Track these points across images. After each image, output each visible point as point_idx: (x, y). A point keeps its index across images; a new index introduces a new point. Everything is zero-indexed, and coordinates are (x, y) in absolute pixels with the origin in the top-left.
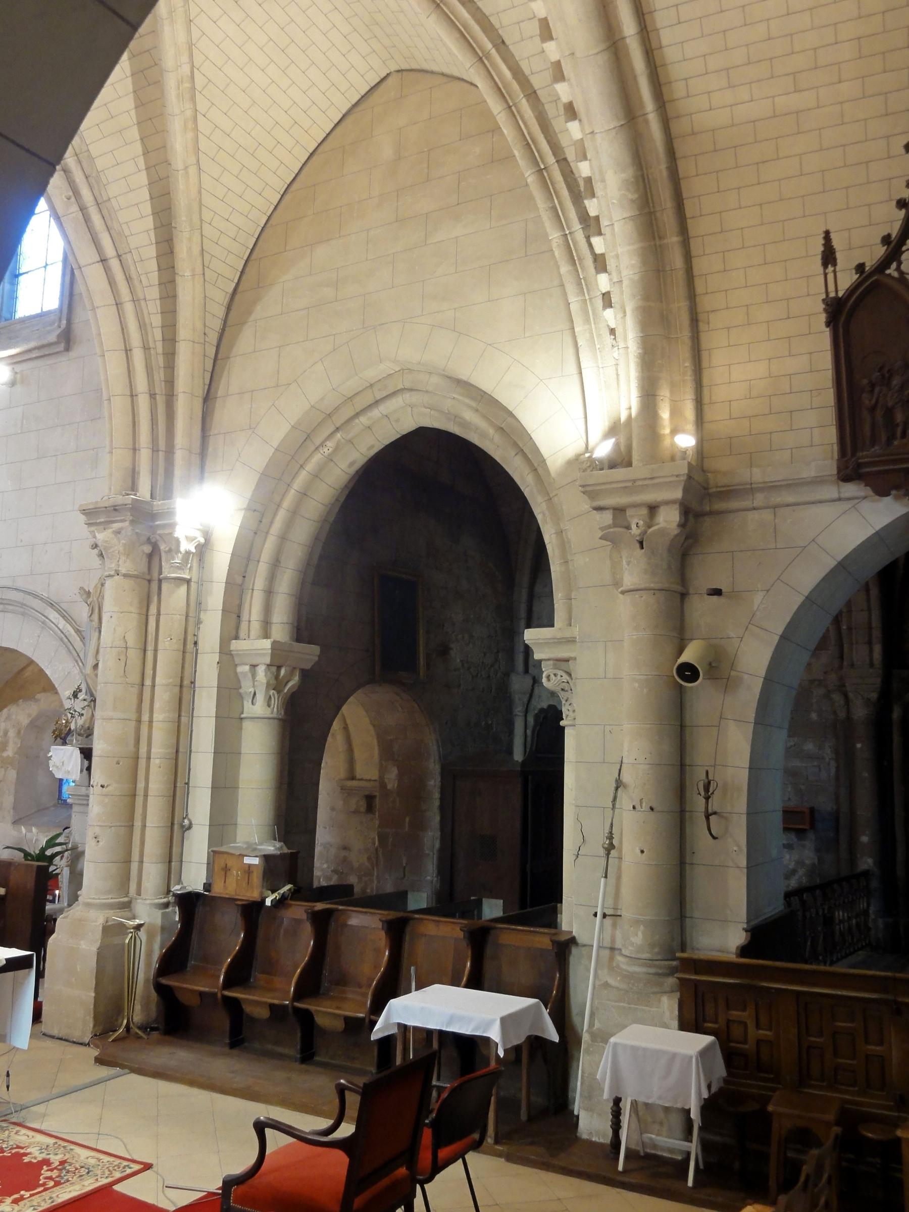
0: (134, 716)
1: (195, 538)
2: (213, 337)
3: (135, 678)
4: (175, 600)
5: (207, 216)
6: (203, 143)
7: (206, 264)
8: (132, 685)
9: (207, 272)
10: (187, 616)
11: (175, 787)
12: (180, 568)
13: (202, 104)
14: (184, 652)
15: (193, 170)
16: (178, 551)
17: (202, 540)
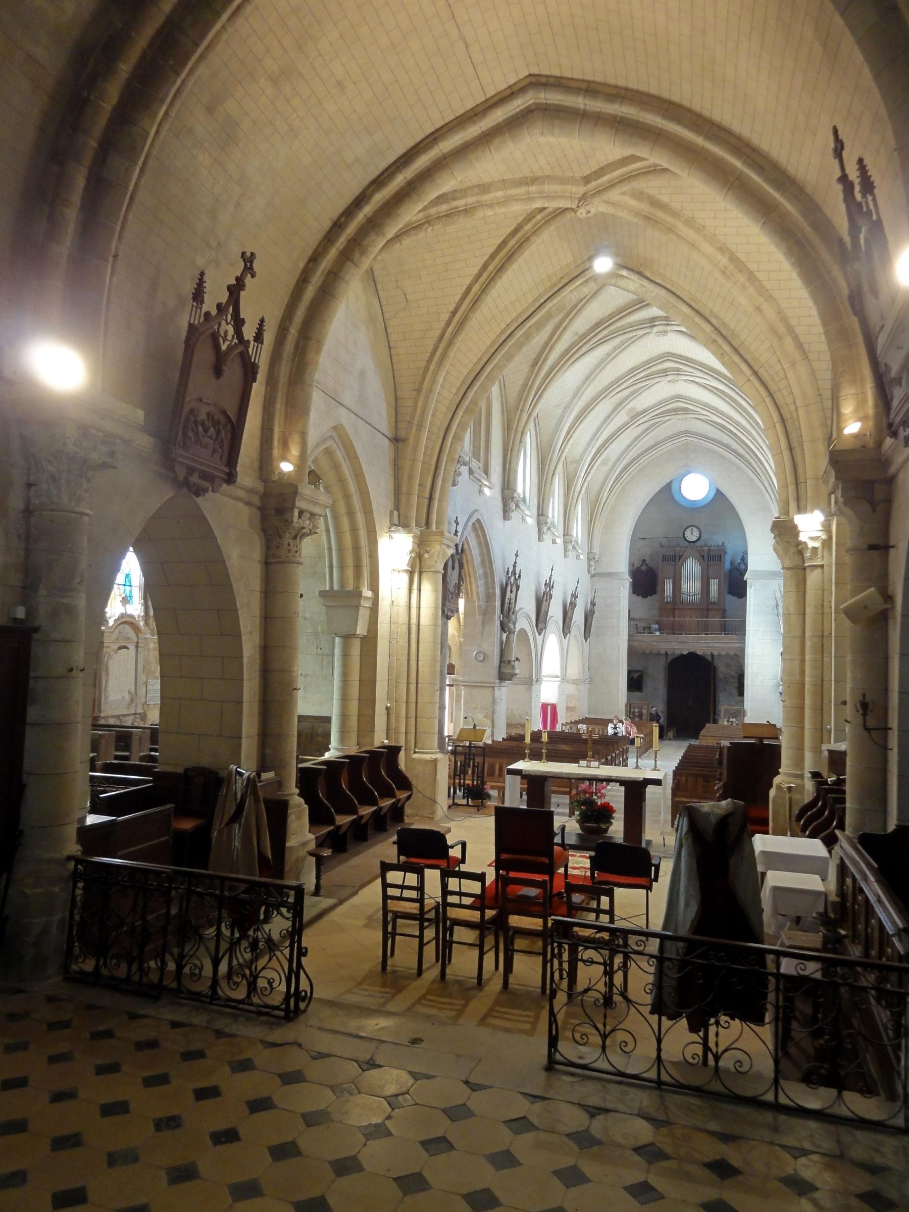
0: (797, 657)
1: (819, 537)
2: (827, 394)
3: (798, 633)
4: (813, 578)
5: (793, 322)
6: (767, 285)
7: (806, 350)
8: (794, 637)
9: (811, 356)
10: (823, 591)
11: (822, 703)
12: (811, 559)
13: (753, 267)
14: (823, 614)
15: (765, 306)
16: (807, 548)
17: (824, 537)
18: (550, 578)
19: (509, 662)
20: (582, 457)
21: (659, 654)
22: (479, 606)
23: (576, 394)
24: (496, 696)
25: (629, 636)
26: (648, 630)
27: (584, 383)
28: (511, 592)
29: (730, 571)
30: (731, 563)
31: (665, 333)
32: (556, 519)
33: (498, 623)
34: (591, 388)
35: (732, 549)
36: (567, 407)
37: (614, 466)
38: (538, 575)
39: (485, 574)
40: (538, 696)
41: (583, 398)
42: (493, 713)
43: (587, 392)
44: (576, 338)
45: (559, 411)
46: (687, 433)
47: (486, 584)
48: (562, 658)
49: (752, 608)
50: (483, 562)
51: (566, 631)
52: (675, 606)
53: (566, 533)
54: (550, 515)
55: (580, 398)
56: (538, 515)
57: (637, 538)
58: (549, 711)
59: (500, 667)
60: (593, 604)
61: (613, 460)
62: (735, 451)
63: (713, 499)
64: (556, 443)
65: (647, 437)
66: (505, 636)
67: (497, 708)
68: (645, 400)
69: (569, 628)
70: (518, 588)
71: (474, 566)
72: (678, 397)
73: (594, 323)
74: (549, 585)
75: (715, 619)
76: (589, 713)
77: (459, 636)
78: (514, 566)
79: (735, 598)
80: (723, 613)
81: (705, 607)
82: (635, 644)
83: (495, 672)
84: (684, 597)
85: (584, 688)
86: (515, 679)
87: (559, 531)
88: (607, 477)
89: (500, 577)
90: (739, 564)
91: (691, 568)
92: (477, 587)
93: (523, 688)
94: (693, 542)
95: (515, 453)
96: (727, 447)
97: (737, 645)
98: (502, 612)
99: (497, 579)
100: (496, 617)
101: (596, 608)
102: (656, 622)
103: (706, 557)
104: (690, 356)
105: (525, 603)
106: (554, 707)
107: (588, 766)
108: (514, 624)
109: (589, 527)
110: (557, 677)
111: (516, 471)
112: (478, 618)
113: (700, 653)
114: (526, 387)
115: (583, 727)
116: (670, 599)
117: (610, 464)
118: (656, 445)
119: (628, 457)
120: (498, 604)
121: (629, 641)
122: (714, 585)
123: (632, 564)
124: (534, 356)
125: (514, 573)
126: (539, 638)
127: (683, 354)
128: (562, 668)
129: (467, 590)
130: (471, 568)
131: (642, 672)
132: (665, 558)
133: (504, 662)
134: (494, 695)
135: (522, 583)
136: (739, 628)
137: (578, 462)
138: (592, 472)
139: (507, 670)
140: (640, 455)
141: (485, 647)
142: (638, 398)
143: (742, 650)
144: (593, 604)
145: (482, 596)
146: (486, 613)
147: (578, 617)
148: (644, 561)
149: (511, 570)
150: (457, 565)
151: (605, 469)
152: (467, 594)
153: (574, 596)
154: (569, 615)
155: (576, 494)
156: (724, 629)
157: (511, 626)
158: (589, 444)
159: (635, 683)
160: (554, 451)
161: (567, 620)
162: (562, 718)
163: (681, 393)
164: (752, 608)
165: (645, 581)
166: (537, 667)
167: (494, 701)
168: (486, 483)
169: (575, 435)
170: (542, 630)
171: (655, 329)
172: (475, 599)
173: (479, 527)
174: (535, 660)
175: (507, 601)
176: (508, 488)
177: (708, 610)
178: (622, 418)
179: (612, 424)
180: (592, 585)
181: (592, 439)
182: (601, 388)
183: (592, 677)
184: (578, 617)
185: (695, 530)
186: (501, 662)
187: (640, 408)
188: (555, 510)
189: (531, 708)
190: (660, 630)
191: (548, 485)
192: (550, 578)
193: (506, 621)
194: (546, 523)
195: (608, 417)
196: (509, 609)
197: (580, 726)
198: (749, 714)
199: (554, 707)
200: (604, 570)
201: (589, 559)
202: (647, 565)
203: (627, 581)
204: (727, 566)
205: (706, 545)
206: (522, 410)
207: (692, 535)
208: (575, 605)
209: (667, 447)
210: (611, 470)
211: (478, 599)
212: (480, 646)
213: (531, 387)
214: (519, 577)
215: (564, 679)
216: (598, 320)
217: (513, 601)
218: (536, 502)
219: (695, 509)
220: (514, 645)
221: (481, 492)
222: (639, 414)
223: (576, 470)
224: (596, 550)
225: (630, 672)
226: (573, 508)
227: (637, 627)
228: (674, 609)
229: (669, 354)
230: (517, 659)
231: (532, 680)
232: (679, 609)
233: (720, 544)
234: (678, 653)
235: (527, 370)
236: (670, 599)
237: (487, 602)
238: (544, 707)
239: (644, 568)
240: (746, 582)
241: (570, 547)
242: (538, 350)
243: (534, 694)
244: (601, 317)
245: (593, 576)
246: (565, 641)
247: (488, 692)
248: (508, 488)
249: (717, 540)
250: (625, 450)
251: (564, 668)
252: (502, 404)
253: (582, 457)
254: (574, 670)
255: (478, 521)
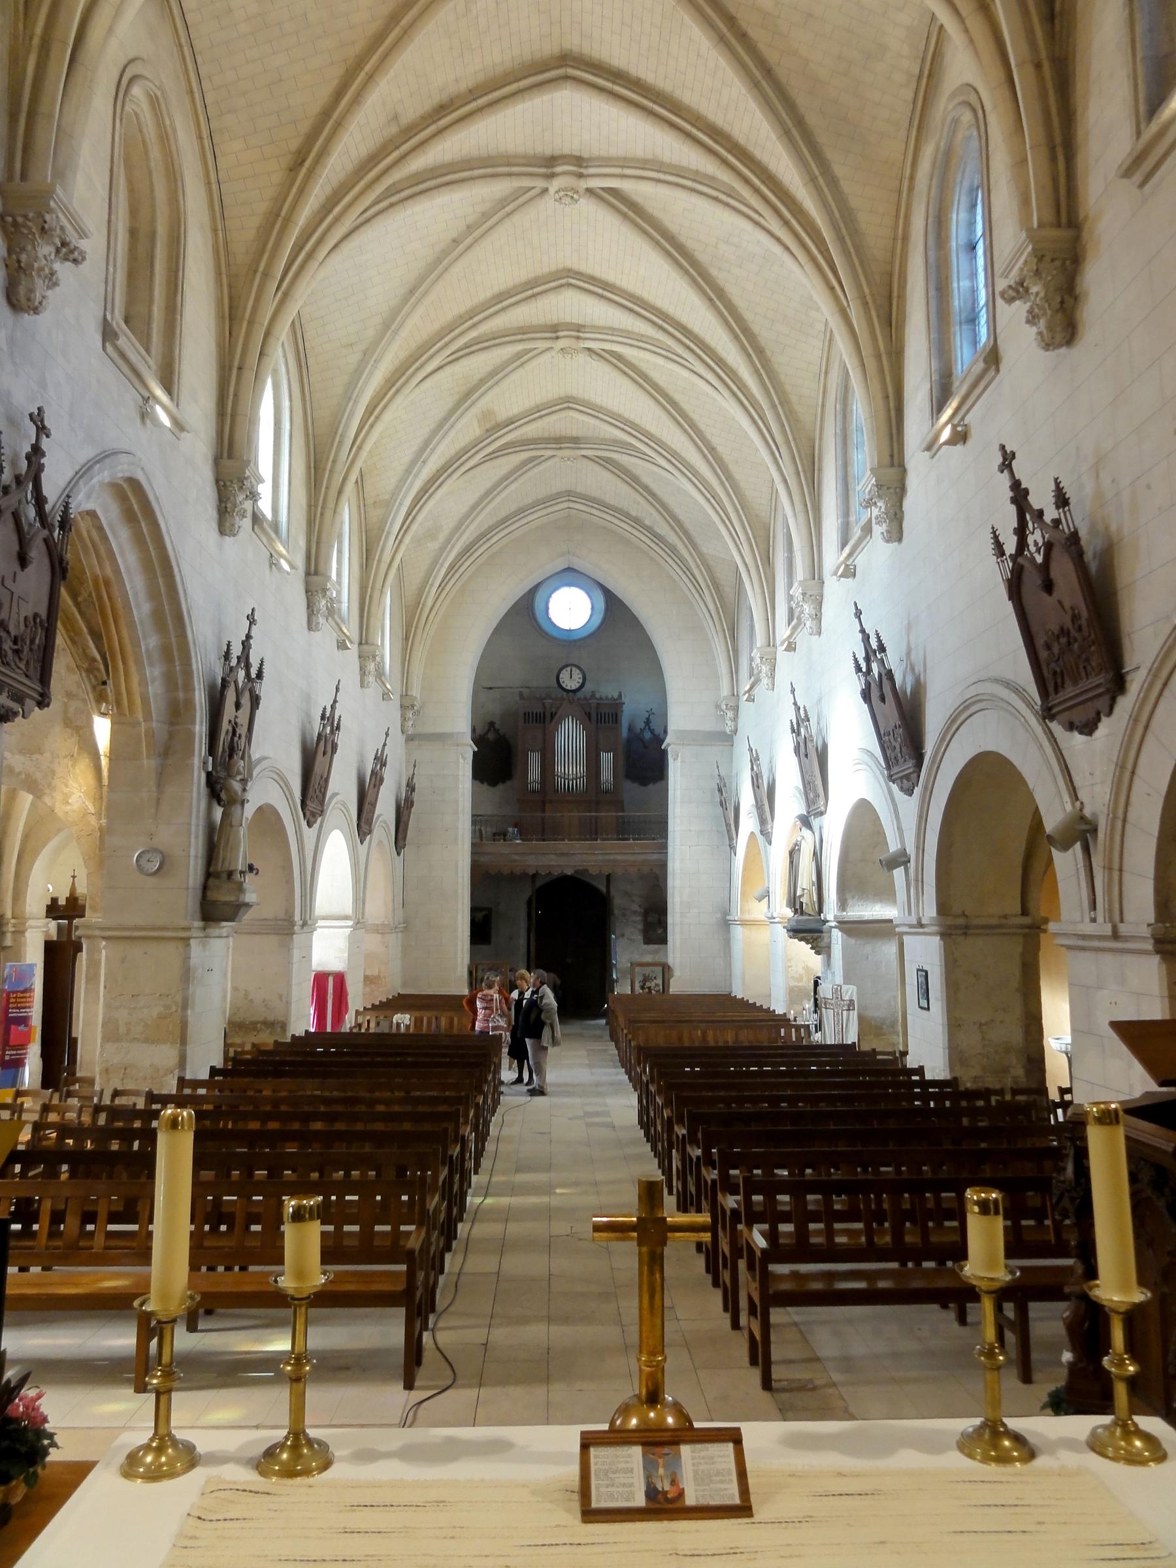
18: (333, 707)
19: (230, 874)
20: (394, 494)
21: (524, 875)
22: (150, 734)
23: (390, 324)
24: (194, 961)
25: (473, 845)
26: (501, 835)
27: (405, 301)
28: (238, 706)
29: (629, 741)
30: (630, 729)
31: (570, 194)
32: (345, 605)
33: (199, 779)
34: (415, 318)
35: (634, 706)
36: (368, 355)
37: (448, 541)
38: (307, 698)
39: (166, 653)
40: (307, 957)
41: (404, 333)
42: (185, 1005)
43: (410, 323)
44: (394, 129)
45: (354, 359)
46: (570, 494)
47: (170, 680)
48: (356, 882)
49: (678, 793)
50: (158, 617)
51: (365, 828)
52: (547, 793)
53: (364, 640)
54: (334, 577)
55: (396, 332)
56: (308, 574)
57: (482, 687)
58: (329, 989)
59: (205, 888)
60: (411, 787)
61: (447, 526)
62: (650, 530)
63: (599, 627)
64: (347, 425)
65: (503, 495)
66: (218, 812)
67: (198, 993)
68: (511, 398)
69: (369, 823)
70: (255, 701)
71: (132, 625)
72: (568, 402)
73: (436, 99)
74: (330, 720)
75: (607, 815)
76: (404, 984)
77: (98, 815)
78: (246, 644)
79: (636, 785)
80: (619, 805)
81: (593, 795)
82: (483, 859)
83: (191, 901)
84: (560, 782)
85: (394, 940)
86: (248, 916)
87: (351, 630)
88: (435, 562)
89: (206, 663)
90: (642, 730)
91: (570, 737)
92: (143, 682)
93: (273, 940)
94: (575, 691)
95: (249, 375)
96: (637, 521)
97: (655, 857)
98: (212, 750)
99: (197, 666)
100: (197, 762)
101: (416, 797)
102: (516, 825)
103: (594, 716)
104: (611, 277)
105: (274, 747)
106: (340, 979)
107: (663, 1506)
108: (244, 782)
109: (404, 649)
110: (346, 918)
111: (253, 421)
112: (149, 764)
113: (594, 871)
114: (276, 219)
115: (403, 1019)
116: (537, 786)
117: (442, 537)
118: (521, 511)
119: (472, 527)
120: (200, 729)
121: (473, 853)
122: (607, 758)
123: (474, 730)
124: (294, 144)
125: (245, 659)
126: (309, 834)
127: (597, 273)
128: (356, 900)
129: (118, 694)
130: (125, 633)
131: (490, 910)
132: (527, 716)
133: (217, 875)
134: (187, 958)
135: (265, 689)
136: (657, 828)
137: (388, 505)
138: (414, 527)
139: (223, 895)
140: (491, 529)
141: (165, 836)
142: (504, 384)
143: (664, 866)
144: (411, 787)
145: (157, 706)
146: (170, 750)
147: (385, 809)
148: (492, 724)
149: (236, 650)
150: (37, 553)
151: (434, 546)
152: (118, 703)
153: (380, 760)
154: (369, 799)
155: (384, 567)
156: (624, 830)
157: (236, 786)
158: (408, 472)
159: (481, 931)
160: (341, 443)
161: (366, 807)
162: (356, 1000)
163: (575, 393)
164: (678, 793)
165: (495, 758)
166: (303, 895)
167: (187, 975)
168: (159, 392)
169: (387, 416)
170: (314, 815)
171: (555, 184)
172: (140, 716)
173: (134, 499)
174: (296, 884)
175: (225, 726)
176: (230, 457)
177: (598, 803)
178: (467, 429)
179: (452, 434)
180: (408, 754)
181: (413, 463)
182: (436, 326)
183: (408, 923)
184: (385, 809)
185: (576, 672)
186: (208, 875)
187: (502, 415)
188: (342, 569)
189: (289, 985)
190: (524, 834)
191: (328, 514)
192: (333, 707)
193: (222, 774)
194: (324, 591)
195: (445, 420)
196: (232, 749)
197: (397, 1018)
198: (677, 973)
199: (340, 979)
200: (429, 729)
201: (403, 707)
202: (497, 731)
203: (468, 750)
204: (625, 733)
205: (593, 695)
206: (266, 275)
207: (571, 681)
208: (381, 781)
209: (537, 518)
210: (442, 549)
211: (148, 716)
212: (151, 836)
213: (288, 221)
214: (260, 675)
215: (359, 922)
216: (445, 97)
217: (242, 730)
218: (302, 543)
219: (570, 643)
220: (242, 831)
221: (145, 415)
222: (499, 427)
223: (383, 522)
224: (415, 692)
225: (474, 910)
226: (377, 594)
227: (486, 831)
228: (544, 803)
229: (570, 273)
230: (251, 868)
231: (292, 924)
232: (551, 802)
233: (616, 695)
234: (556, 873)
235: (277, 178)
236: (537, 786)
237: (172, 724)
238: (320, 979)
239: (491, 736)
240: (664, 754)
241: (371, 667)
242: (305, 127)
243: (296, 954)
244: (453, 90)
245: (410, 739)
246: (362, 849)
247: (170, 952)
248: (230, 457)
249: (608, 691)
250: (467, 516)
251: (360, 899)
252: (216, 251)
253: (394, 494)
254: (379, 907)
255: (134, 483)
